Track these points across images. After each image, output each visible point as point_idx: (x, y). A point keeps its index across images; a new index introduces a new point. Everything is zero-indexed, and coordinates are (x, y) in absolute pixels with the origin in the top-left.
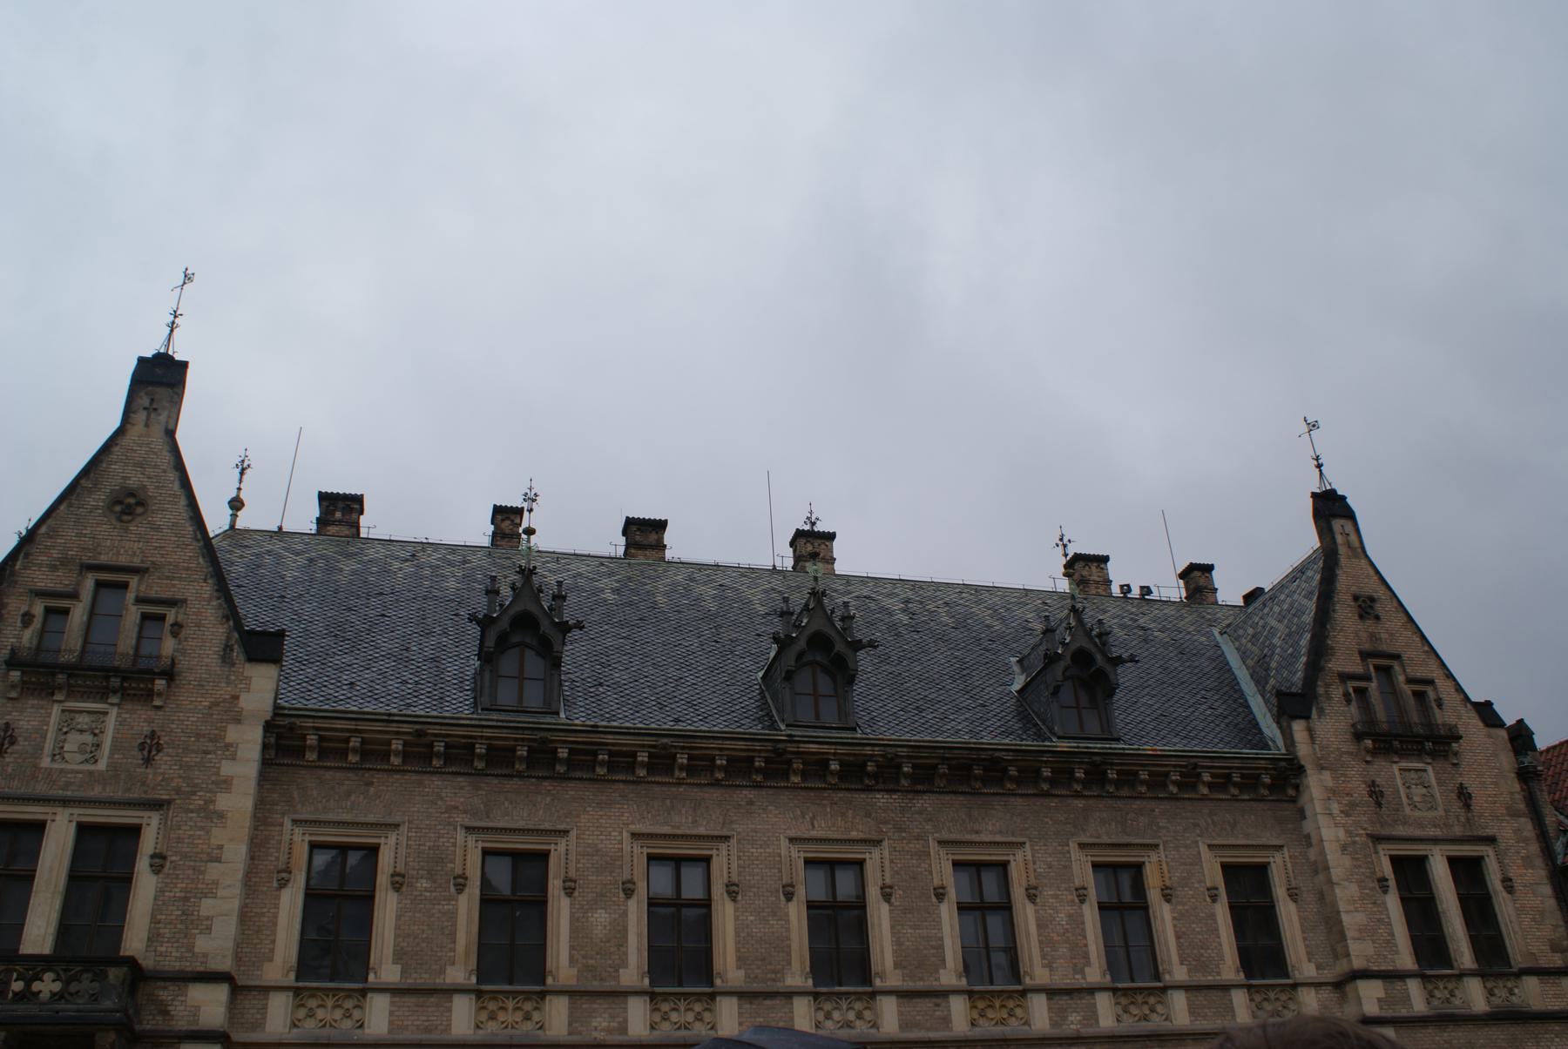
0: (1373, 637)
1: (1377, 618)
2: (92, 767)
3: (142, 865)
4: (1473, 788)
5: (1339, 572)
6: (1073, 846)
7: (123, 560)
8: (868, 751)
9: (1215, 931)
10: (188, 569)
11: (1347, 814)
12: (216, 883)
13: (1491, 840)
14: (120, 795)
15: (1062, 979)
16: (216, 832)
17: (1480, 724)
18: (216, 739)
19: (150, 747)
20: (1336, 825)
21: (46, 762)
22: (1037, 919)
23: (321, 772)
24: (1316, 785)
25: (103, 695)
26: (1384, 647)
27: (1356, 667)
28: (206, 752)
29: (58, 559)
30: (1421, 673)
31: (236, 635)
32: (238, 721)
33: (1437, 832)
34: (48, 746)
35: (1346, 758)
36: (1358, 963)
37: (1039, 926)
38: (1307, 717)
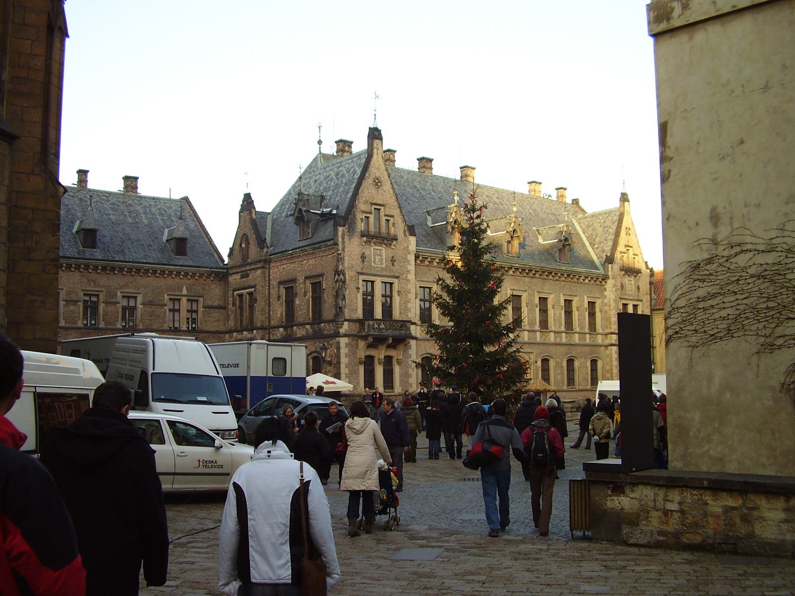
1: (629, 235)
2: (382, 266)
3: (395, 294)
4: (640, 287)
5: (624, 220)
6: (561, 295)
7: (379, 202)
8: (527, 267)
9: (585, 319)
10: (393, 205)
12: (410, 299)
13: (641, 301)
14: (389, 274)
15: (558, 330)
16: (408, 285)
18: (406, 259)
19: (393, 261)
20: (614, 294)
21: (373, 264)
22: (554, 313)
23: (420, 266)
24: (610, 282)
25: (380, 244)
27: (624, 250)
28: (404, 263)
29: (365, 201)
31: (406, 227)
32: (409, 254)
33: (631, 298)
34: (372, 259)
35: (618, 276)
37: (554, 315)
38: (612, 264)
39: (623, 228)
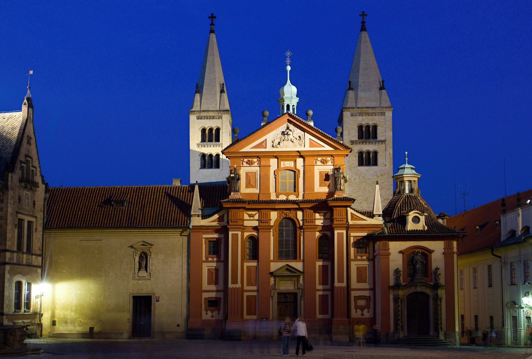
0: (29, 150)
1: (30, 144)
11: (13, 204)
17: (41, 183)
26: (30, 155)
30: (34, 165)
33: (27, 213)
36: (7, 248)
39: (25, 136)
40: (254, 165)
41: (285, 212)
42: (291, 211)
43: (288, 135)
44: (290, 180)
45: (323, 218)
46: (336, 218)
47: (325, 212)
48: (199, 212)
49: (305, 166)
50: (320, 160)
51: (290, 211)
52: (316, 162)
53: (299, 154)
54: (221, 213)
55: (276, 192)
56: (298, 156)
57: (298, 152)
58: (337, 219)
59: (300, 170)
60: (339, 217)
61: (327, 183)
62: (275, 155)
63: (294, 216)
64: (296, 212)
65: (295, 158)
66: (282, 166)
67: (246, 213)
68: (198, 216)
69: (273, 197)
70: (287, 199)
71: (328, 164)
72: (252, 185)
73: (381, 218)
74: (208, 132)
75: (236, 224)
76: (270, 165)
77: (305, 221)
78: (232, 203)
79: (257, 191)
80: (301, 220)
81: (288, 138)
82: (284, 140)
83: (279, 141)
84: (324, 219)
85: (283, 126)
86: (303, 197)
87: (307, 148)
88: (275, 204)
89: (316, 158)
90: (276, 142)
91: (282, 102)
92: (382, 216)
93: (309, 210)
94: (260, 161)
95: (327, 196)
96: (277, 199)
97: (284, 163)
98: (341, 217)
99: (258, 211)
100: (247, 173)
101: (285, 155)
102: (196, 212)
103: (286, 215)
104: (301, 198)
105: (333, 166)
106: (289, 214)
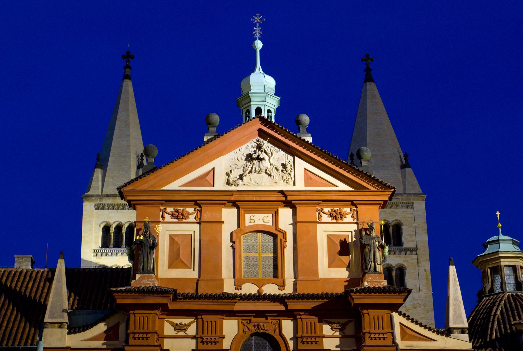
40: (188, 220)
41: (254, 320)
42: (269, 318)
43: (259, 162)
44: (265, 252)
45: (340, 334)
46: (369, 333)
47: (343, 321)
48: (63, 317)
49: (298, 224)
50: (329, 212)
51: (267, 319)
52: (320, 215)
53: (283, 199)
54: (113, 320)
55: (234, 277)
56: (282, 201)
57: (282, 192)
58: (373, 335)
59: (285, 232)
60: (377, 330)
61: (346, 259)
62: (233, 199)
63: (275, 330)
64: (279, 320)
65: (274, 208)
66: (248, 223)
67: (168, 322)
68: (61, 325)
69: (229, 288)
70: (258, 291)
71: (345, 220)
72: (184, 263)
73: (466, 336)
74: (115, 232)
75: (145, 342)
76: (223, 220)
77: (300, 340)
78: (137, 294)
79: (194, 274)
80: (291, 339)
81: (259, 167)
82: (250, 172)
83: (241, 172)
84: (341, 336)
85: (249, 144)
86: (295, 289)
87: (301, 185)
88: (234, 301)
89: (320, 208)
90: (235, 175)
91: (246, 104)
92: (467, 331)
93: (308, 316)
94: (201, 212)
95: (345, 286)
96: (237, 291)
97: (252, 218)
98: (381, 330)
99: (197, 319)
100: (172, 236)
101: (254, 200)
102: (55, 318)
103: (258, 327)
104: (289, 290)
105: (356, 225)
106: (263, 325)
